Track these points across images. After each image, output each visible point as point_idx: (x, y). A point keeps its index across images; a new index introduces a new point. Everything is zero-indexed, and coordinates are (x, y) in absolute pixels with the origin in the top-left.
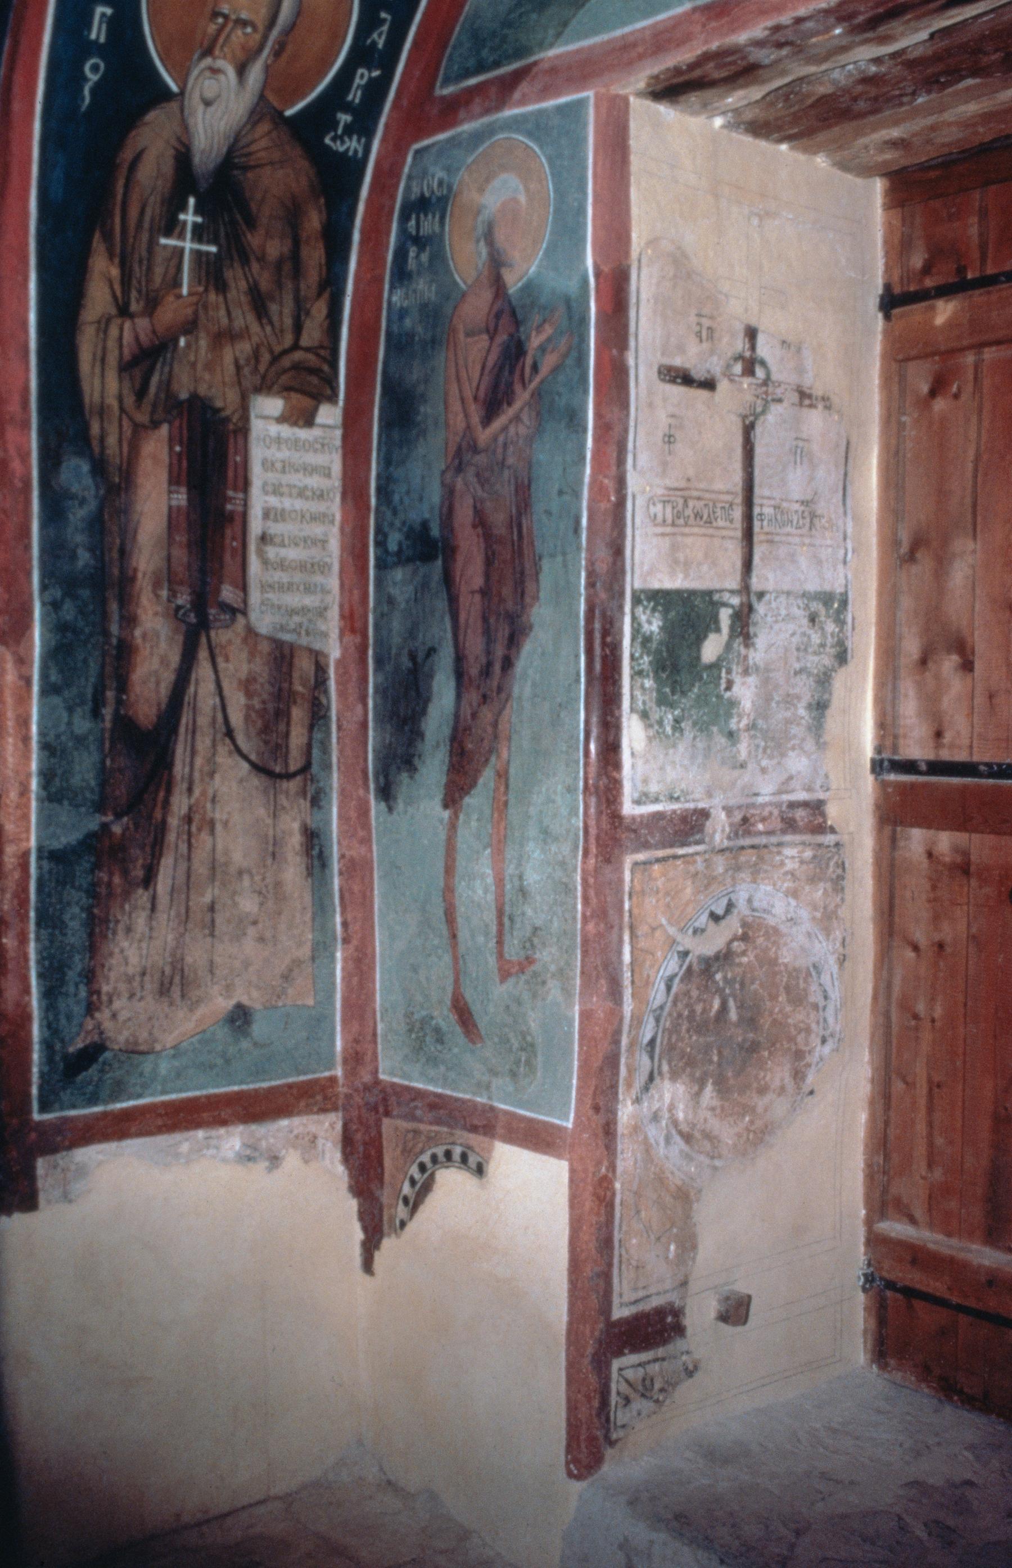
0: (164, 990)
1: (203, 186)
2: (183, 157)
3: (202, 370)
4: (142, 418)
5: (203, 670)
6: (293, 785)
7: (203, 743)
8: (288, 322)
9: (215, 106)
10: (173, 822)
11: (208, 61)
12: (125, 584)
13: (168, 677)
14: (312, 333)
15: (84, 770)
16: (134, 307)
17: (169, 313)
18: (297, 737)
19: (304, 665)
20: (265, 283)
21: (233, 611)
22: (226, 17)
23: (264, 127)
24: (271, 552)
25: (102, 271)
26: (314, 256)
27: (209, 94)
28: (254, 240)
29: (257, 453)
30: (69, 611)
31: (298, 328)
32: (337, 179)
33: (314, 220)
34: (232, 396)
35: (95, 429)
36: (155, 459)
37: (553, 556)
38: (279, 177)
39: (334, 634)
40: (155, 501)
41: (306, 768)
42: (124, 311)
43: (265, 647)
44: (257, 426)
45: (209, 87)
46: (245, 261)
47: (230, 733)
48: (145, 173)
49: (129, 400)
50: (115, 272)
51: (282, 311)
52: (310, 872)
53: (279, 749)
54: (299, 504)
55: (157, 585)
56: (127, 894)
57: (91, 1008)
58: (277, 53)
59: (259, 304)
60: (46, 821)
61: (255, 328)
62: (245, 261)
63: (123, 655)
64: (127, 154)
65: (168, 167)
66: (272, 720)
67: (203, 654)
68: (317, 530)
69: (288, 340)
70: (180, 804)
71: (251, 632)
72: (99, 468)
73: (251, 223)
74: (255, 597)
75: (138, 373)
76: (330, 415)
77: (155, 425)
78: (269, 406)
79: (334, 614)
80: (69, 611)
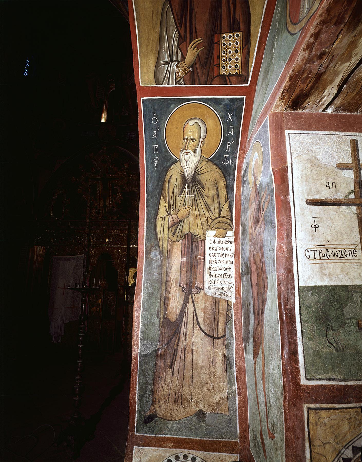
0: (176, 401)
1: (189, 181)
2: (183, 176)
3: (191, 226)
4: (174, 239)
5: (190, 305)
6: (220, 341)
7: (190, 327)
8: (217, 211)
9: (189, 161)
10: (180, 349)
11: (185, 151)
12: (167, 282)
13: (179, 308)
14: (225, 212)
15: (155, 332)
16: (172, 213)
17: (182, 213)
18: (221, 326)
19: (223, 305)
20: (209, 201)
21: (200, 289)
22: (187, 139)
23: (204, 163)
24: (212, 272)
25: (163, 204)
26: (223, 192)
27: (186, 159)
28: (205, 192)
29: (208, 245)
30: (151, 289)
31: (220, 212)
32: (227, 172)
33: (222, 184)
34: (200, 232)
35: (161, 243)
36: (178, 248)
37: (269, 273)
38: (211, 175)
39: (234, 296)
40: (177, 260)
41: (224, 336)
42: (169, 214)
43: (210, 299)
44: (208, 239)
45: (187, 157)
46: (202, 196)
47: (198, 324)
48: (173, 181)
49: (171, 235)
50: (167, 205)
51: (215, 208)
52: (226, 369)
53: (215, 329)
54: (221, 259)
55: (176, 282)
56: (165, 369)
57: (153, 403)
58: (203, 144)
59: (208, 208)
60: (143, 345)
61: (207, 213)
62: (202, 196)
63: (166, 300)
64: (168, 177)
65: (179, 178)
66: (213, 320)
67: (190, 301)
68: (226, 266)
69: (217, 215)
70: (182, 343)
71: (205, 295)
72: (161, 253)
73: (203, 188)
74: (207, 285)
75: (173, 228)
76: (231, 233)
77: (178, 241)
78: (211, 233)
79: (233, 290)
80: (151, 289)
